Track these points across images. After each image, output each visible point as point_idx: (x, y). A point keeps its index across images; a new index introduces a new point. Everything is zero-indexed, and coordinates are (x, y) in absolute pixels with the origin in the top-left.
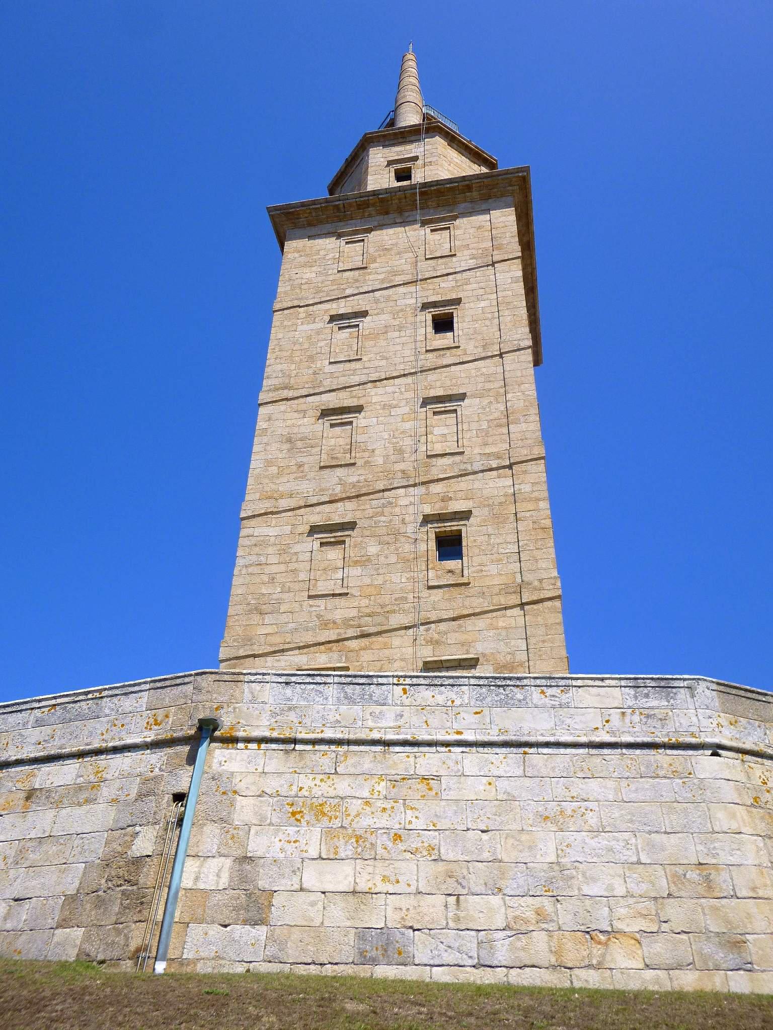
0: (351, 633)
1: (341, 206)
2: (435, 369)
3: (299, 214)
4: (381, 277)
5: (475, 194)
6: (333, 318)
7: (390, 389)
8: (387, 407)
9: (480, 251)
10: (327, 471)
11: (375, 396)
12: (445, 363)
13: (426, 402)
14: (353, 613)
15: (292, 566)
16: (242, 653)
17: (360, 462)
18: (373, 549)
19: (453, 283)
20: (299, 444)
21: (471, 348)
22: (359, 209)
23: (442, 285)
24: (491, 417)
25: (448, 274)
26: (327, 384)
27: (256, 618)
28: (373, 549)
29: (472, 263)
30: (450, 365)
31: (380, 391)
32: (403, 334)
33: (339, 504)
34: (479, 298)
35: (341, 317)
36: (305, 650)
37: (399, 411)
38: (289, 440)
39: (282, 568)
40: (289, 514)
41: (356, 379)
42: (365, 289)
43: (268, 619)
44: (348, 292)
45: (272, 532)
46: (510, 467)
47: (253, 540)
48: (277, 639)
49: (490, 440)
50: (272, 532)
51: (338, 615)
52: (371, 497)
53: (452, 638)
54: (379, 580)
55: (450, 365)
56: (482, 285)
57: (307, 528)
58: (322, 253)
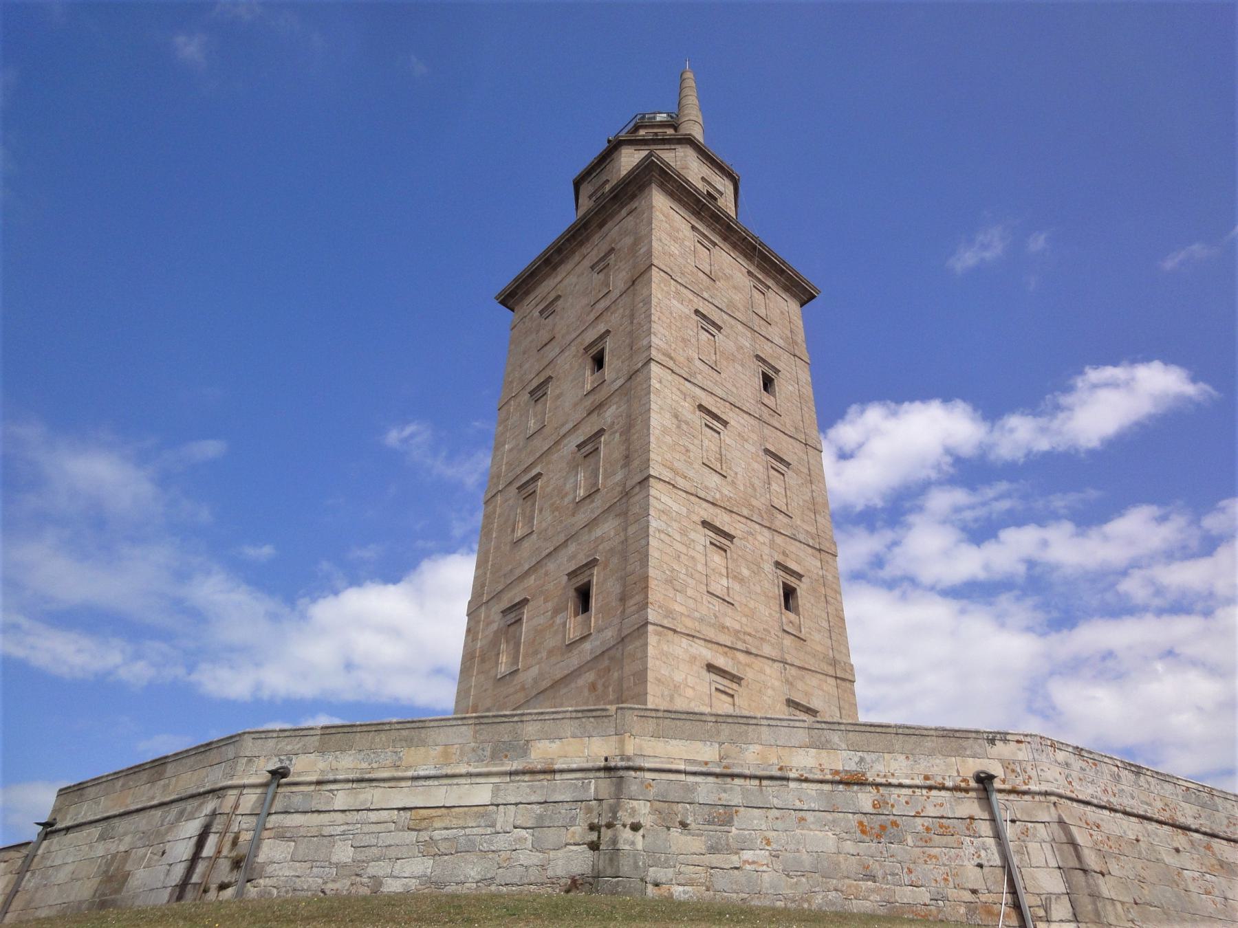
0: (740, 645)
6: (697, 312)
10: (706, 470)
13: (767, 451)
14: (737, 627)
15: (692, 553)
16: (666, 623)
17: (729, 478)
18: (746, 572)
20: (684, 426)
26: (699, 379)
27: (671, 593)
28: (746, 572)
33: (718, 511)
36: (710, 645)
38: (676, 417)
39: (684, 550)
40: (684, 495)
43: (679, 597)
45: (675, 507)
46: (820, 550)
47: (661, 507)
48: (689, 623)
49: (806, 518)
50: (675, 507)
51: (728, 622)
52: (739, 518)
53: (800, 685)
54: (752, 604)
57: (698, 519)
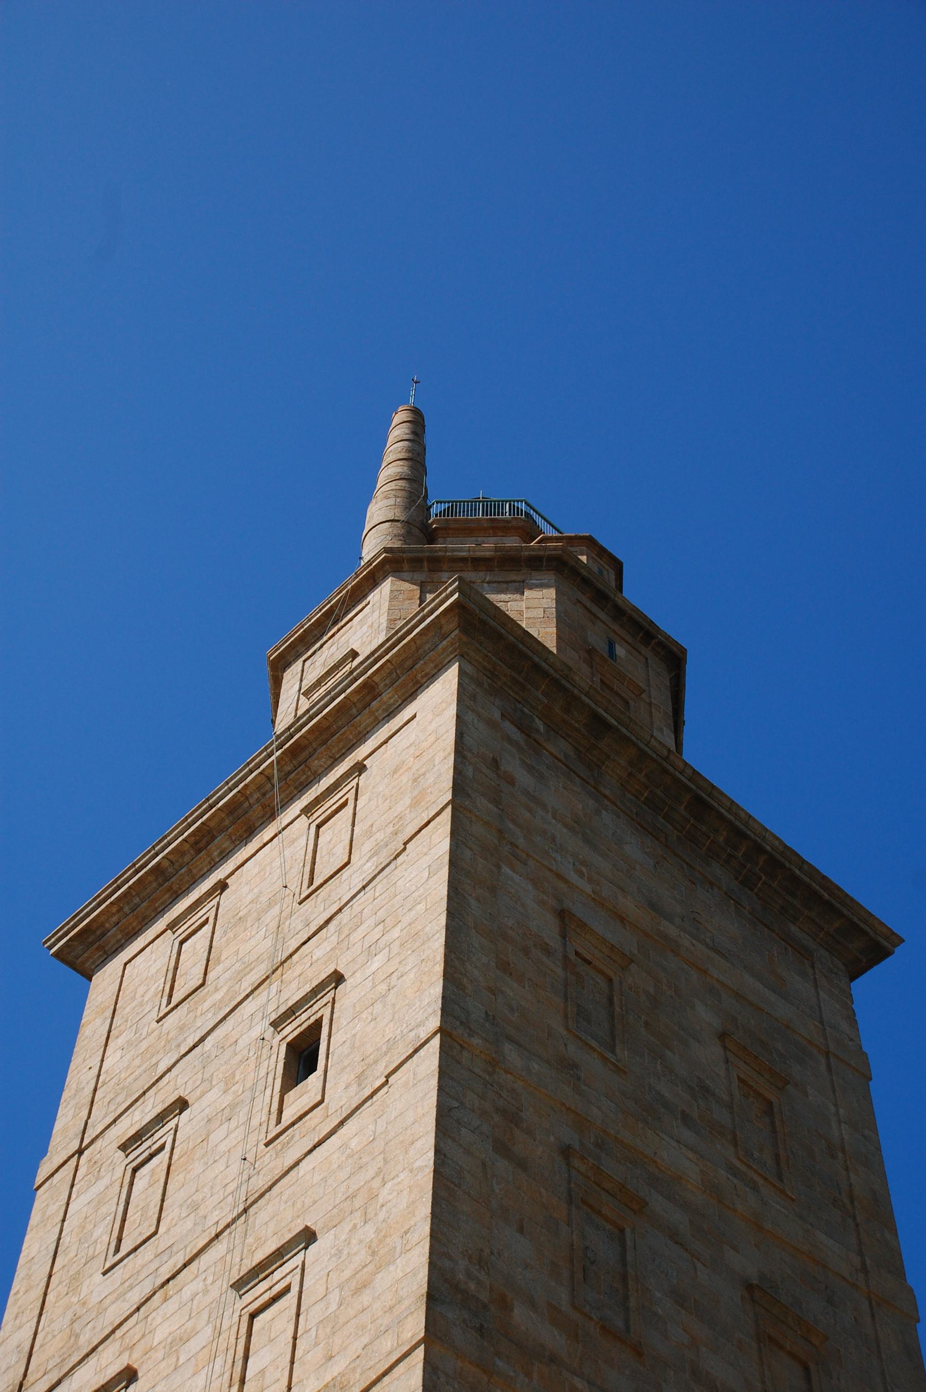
1: (166, 863)
2: (270, 1188)
3: (102, 925)
4: (218, 996)
5: (387, 696)
7: (187, 1293)
8: (178, 1341)
9: (390, 829)
11: (165, 1320)
12: (289, 1162)
19: (334, 939)
21: (340, 1097)
22: (199, 851)
23: (318, 954)
24: (347, 1273)
25: (328, 922)
29: (370, 868)
30: (297, 1164)
31: (171, 1306)
32: (233, 1123)
34: (371, 952)
35: (138, 1137)
37: (194, 1345)
41: (135, 1297)
42: (191, 1043)
44: (162, 1068)
55: (297, 1164)
56: (381, 914)
58: (141, 990)
